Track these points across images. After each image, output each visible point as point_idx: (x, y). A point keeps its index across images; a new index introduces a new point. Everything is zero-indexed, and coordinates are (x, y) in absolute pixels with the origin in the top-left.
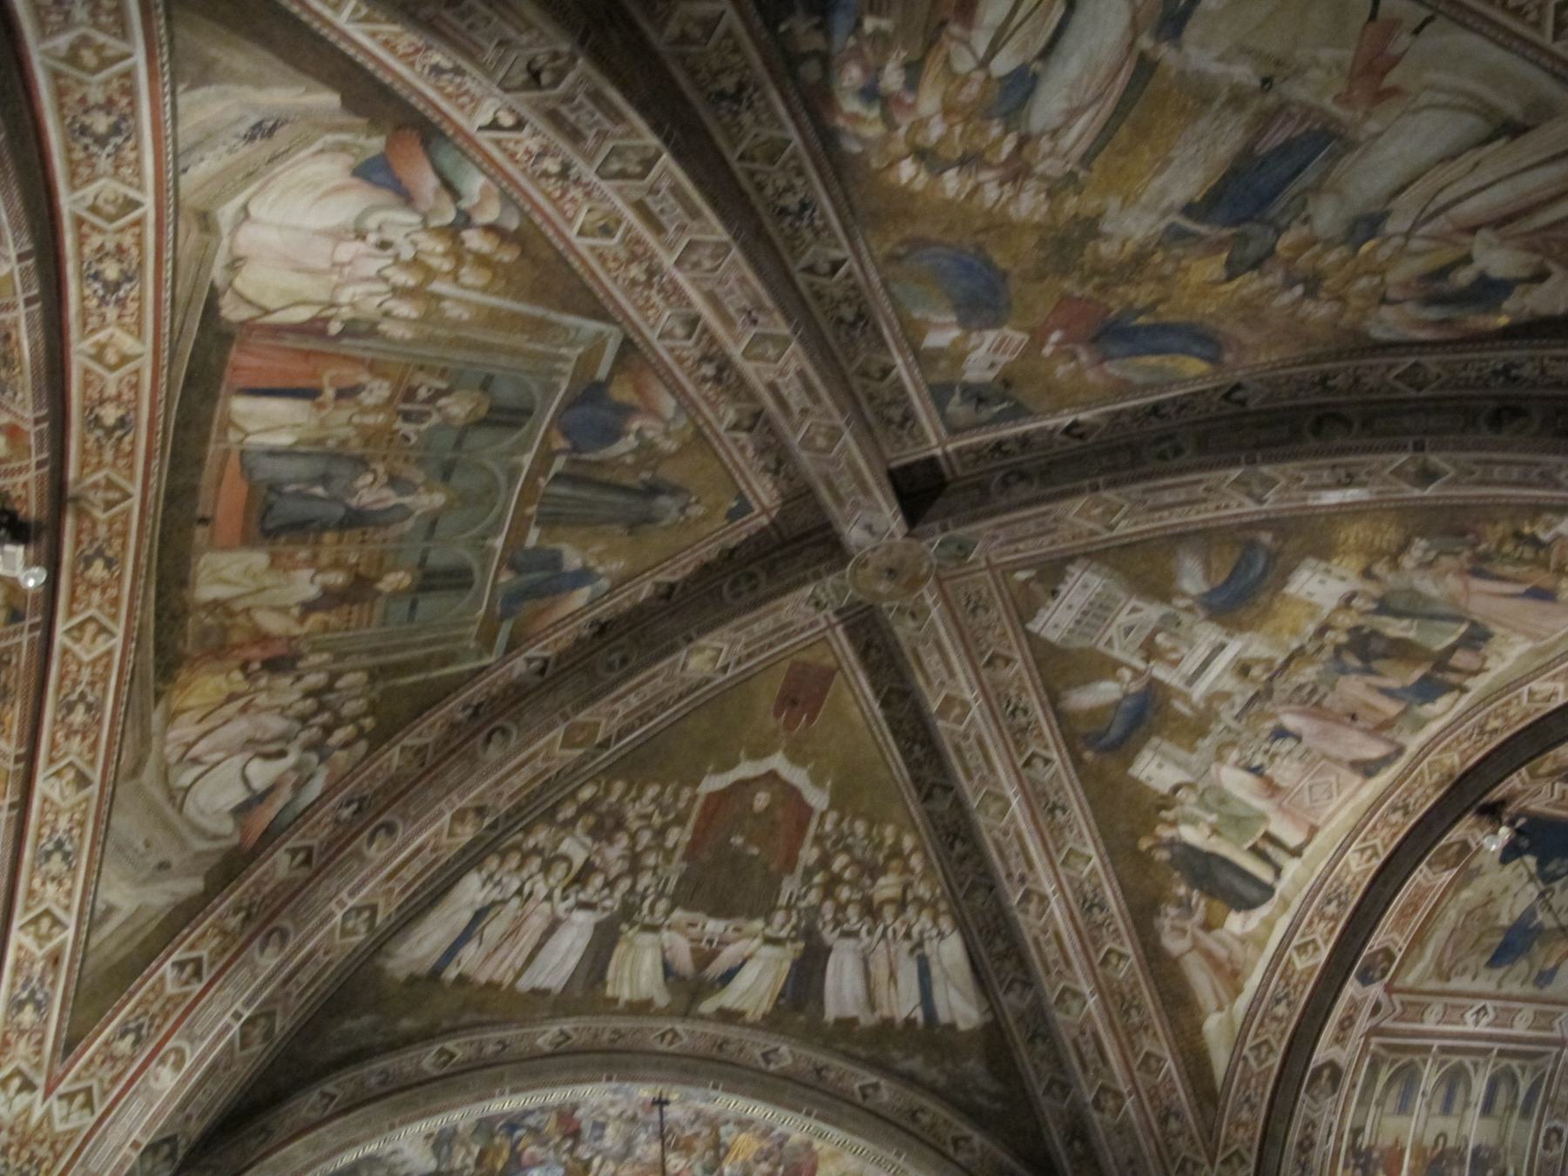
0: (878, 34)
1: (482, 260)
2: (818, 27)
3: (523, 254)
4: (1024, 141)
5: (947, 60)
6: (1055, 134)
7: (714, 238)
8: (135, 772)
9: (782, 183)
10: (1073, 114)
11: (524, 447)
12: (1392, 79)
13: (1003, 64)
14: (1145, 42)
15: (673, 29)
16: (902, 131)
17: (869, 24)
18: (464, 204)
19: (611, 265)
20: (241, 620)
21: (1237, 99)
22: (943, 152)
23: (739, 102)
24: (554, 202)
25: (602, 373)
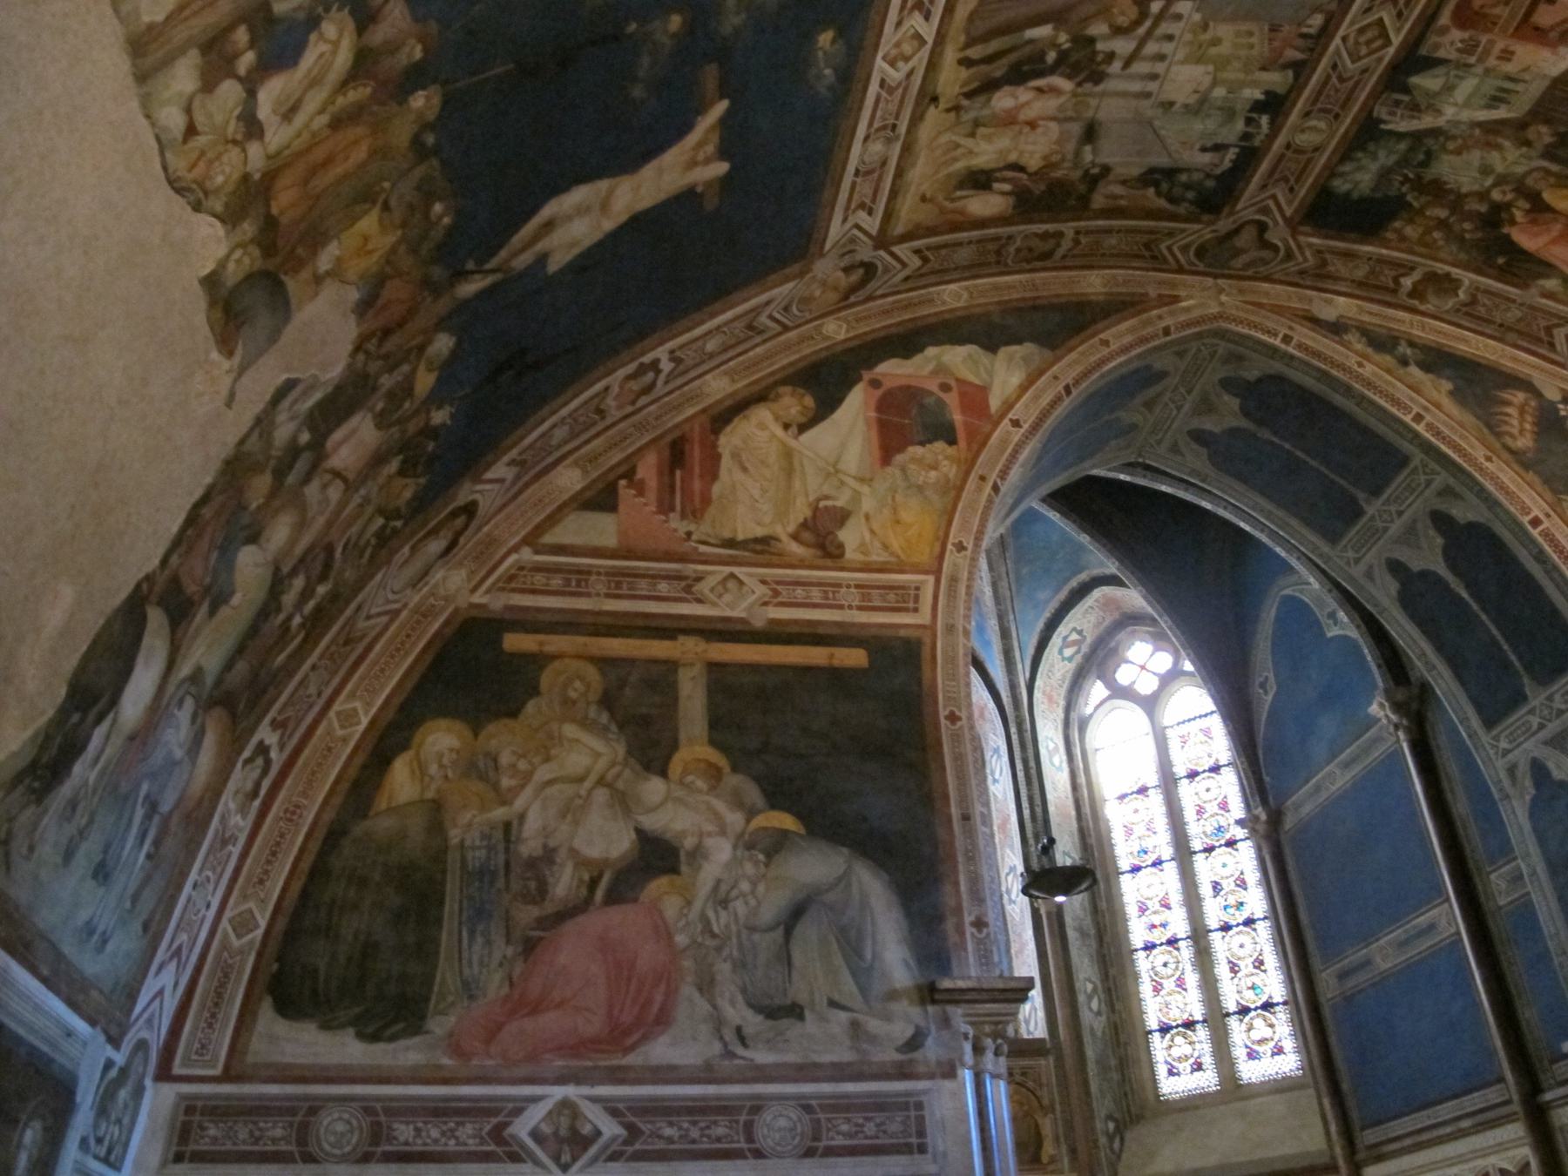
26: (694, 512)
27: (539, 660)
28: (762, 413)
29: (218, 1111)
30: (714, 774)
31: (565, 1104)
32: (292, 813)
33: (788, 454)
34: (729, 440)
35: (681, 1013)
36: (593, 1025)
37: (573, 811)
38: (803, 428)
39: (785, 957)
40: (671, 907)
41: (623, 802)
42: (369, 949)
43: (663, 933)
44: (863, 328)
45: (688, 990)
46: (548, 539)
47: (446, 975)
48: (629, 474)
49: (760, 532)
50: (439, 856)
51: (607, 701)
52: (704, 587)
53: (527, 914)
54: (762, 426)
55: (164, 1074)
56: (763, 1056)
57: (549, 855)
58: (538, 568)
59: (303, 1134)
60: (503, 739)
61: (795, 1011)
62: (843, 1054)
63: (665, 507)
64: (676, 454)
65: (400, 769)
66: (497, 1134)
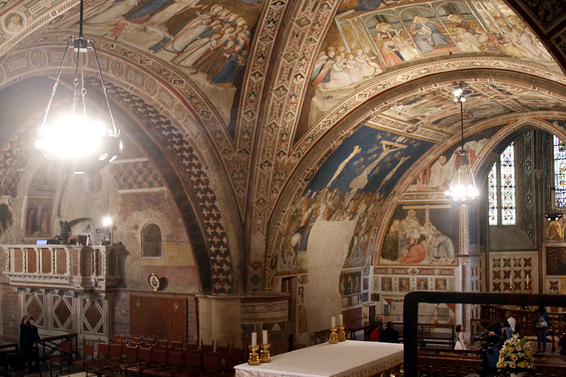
0: (228, 54)
1: (336, 50)
2: (237, 60)
3: (329, 46)
4: (209, 24)
5: (217, 44)
6: (201, 24)
7: (285, 60)
8: (546, 67)
9: (269, 30)
10: (195, 27)
11: (389, 12)
12: (113, 27)
13: (207, 40)
14: (172, 38)
15: (260, 79)
16: (236, 32)
17: (228, 56)
18: (325, 62)
19: (319, 32)
20: (484, 44)
21: (153, 24)
22: (230, 25)
23: (262, 54)
24: (311, 53)
25: (353, 11)
26: (427, 184)
27: (408, 210)
28: (438, 162)
29: (377, 268)
30: (430, 226)
31: (413, 268)
32: (381, 234)
33: (441, 170)
34: (433, 168)
35: (426, 258)
36: (416, 259)
37: (412, 232)
38: (444, 164)
39: (438, 251)
40: (424, 244)
41: (419, 230)
42: (391, 250)
43: (424, 248)
44: (455, 141)
45: (427, 255)
46: (408, 190)
47: (399, 254)
48: (418, 177)
49: (437, 186)
50: (397, 238)
51: (416, 216)
52: (429, 196)
53: (407, 246)
54: (438, 165)
55: (372, 265)
56: (435, 263)
57: (410, 238)
58: (407, 195)
59: (386, 271)
60: (404, 222)
61: (439, 258)
62: (445, 264)
63: (423, 183)
64: (425, 172)
65: (392, 227)
66: (406, 272)
